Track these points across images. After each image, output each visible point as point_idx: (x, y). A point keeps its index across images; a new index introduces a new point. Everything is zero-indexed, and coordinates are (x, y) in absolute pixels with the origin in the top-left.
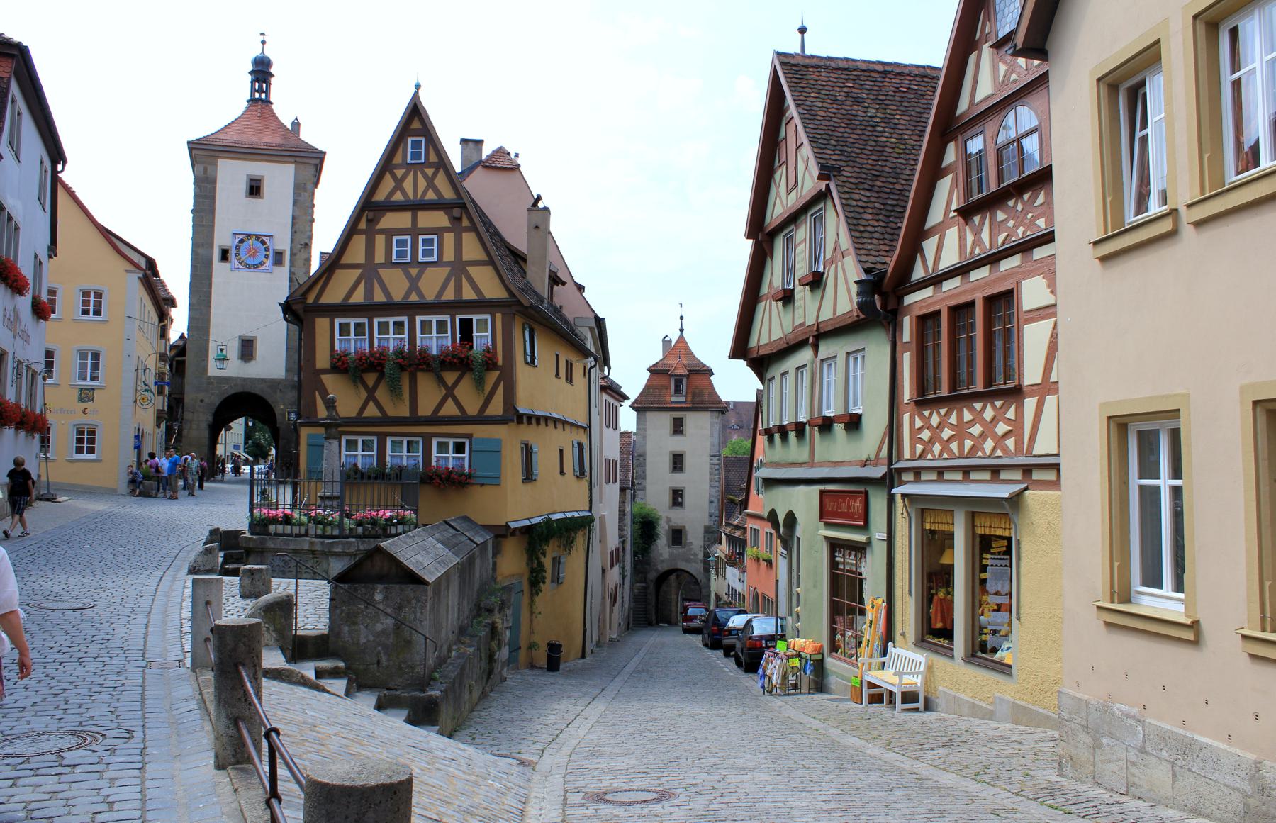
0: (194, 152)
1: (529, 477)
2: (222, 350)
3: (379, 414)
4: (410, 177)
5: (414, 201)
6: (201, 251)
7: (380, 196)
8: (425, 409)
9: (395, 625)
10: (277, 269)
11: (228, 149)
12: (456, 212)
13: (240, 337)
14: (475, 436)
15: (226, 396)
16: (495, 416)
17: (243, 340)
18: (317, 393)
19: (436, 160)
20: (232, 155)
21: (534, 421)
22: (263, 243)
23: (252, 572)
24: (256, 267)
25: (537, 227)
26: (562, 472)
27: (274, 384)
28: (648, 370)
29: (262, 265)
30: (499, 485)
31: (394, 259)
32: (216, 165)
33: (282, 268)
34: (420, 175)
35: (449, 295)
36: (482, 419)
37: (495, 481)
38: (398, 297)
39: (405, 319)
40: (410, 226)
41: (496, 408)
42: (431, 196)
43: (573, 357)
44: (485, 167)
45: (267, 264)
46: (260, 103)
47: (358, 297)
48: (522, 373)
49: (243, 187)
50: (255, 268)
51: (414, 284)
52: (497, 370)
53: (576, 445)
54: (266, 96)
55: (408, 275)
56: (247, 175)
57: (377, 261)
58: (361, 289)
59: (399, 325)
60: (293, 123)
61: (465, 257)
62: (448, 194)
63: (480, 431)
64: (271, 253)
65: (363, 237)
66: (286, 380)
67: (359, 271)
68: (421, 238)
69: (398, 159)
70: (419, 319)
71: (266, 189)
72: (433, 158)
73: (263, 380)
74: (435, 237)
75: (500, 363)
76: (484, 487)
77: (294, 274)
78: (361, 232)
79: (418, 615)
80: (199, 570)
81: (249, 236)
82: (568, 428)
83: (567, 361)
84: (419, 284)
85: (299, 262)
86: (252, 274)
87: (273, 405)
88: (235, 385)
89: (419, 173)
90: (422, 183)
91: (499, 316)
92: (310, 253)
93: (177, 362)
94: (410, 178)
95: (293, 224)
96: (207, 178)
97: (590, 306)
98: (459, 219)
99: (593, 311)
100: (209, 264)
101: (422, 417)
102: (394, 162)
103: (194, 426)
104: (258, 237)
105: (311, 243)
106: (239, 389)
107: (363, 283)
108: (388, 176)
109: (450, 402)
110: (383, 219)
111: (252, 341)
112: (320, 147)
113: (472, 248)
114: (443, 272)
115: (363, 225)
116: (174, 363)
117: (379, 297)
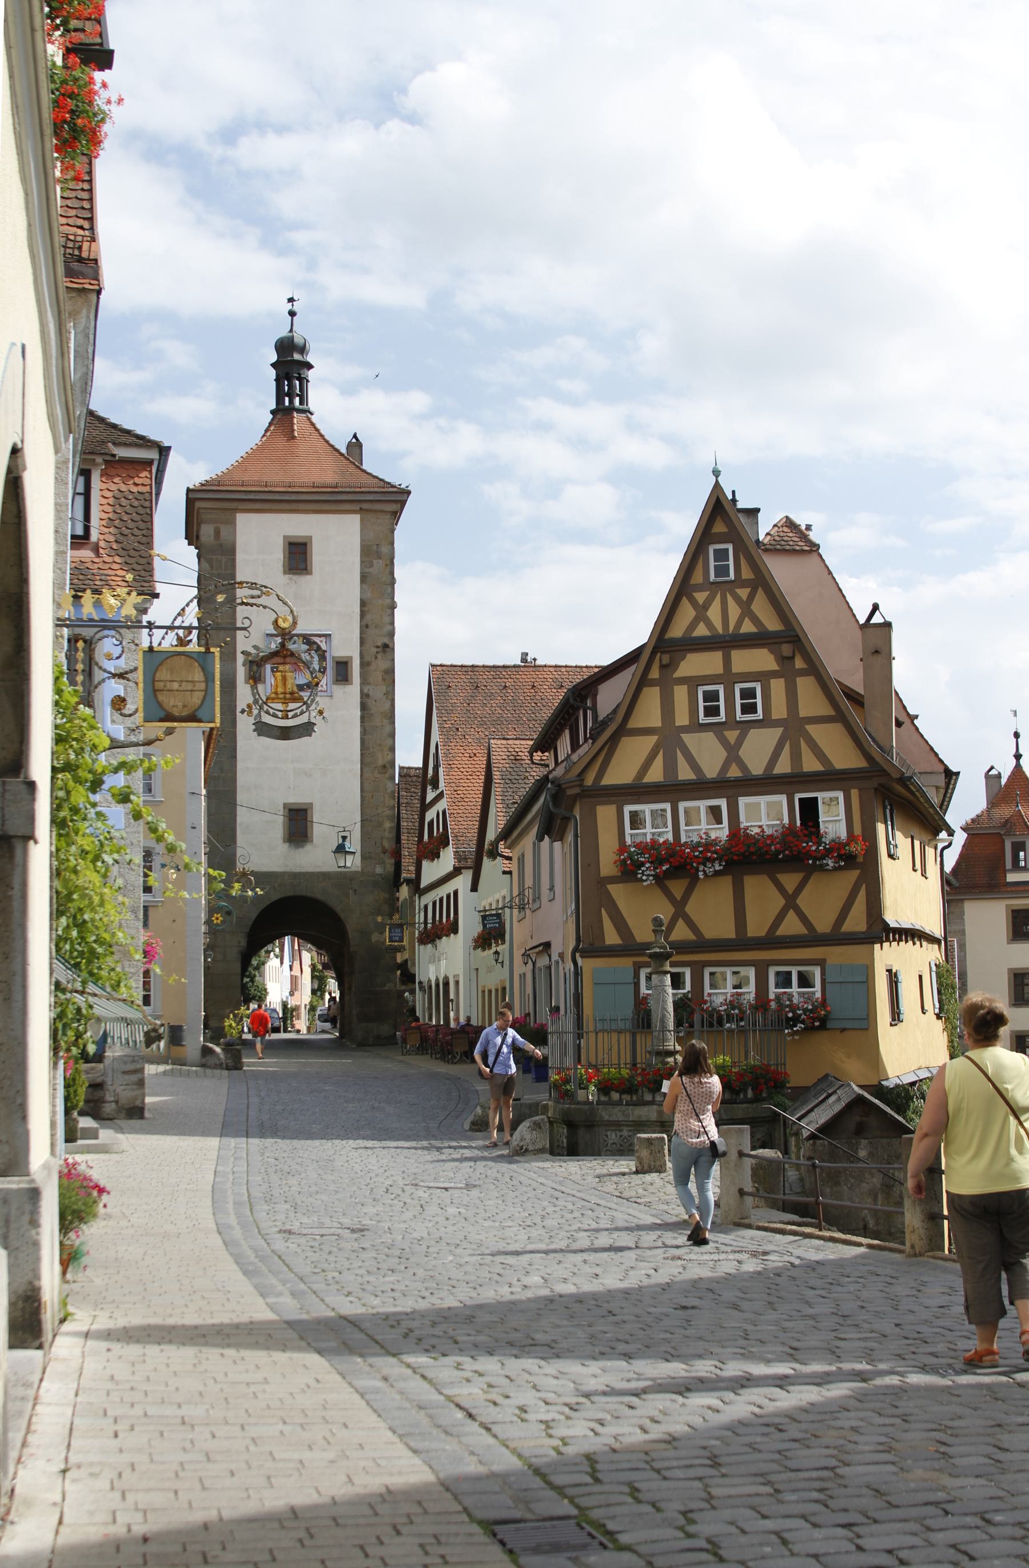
1: (896, 1017)
2: (344, 838)
4: (716, 604)
5: (723, 636)
7: (677, 631)
8: (756, 928)
10: (338, 690)
11: (252, 496)
12: (786, 649)
13: (285, 805)
15: (268, 903)
17: (290, 810)
20: (258, 506)
25: (876, 652)
27: (342, 880)
32: (233, 523)
33: (348, 688)
35: (783, 766)
36: (837, 938)
37: (867, 1024)
38: (711, 771)
39: (723, 803)
40: (720, 670)
41: (856, 922)
42: (748, 627)
45: (323, 682)
46: (295, 414)
47: (656, 774)
49: (278, 556)
51: (733, 752)
52: (857, 869)
53: (934, 968)
54: (301, 403)
55: (724, 742)
56: (284, 537)
57: (679, 722)
58: (659, 762)
59: (715, 813)
60: (350, 445)
61: (802, 713)
62: (773, 624)
63: (835, 955)
64: (330, 665)
65: (657, 689)
66: (362, 872)
67: (655, 738)
68: (738, 688)
69: (697, 578)
70: (743, 801)
71: (317, 556)
72: (747, 574)
77: (368, 696)
78: (653, 683)
80: (527, 1150)
84: (740, 753)
85: (377, 676)
87: (342, 916)
89: (729, 597)
90: (734, 611)
91: (854, 793)
92: (393, 660)
94: (716, 604)
95: (363, 615)
97: (936, 755)
98: (792, 658)
101: (753, 938)
102: (693, 582)
106: (290, 893)
107: (661, 753)
108: (685, 602)
109: (791, 914)
110: (682, 664)
111: (306, 810)
114: (770, 737)
115: (655, 673)
117: (685, 773)
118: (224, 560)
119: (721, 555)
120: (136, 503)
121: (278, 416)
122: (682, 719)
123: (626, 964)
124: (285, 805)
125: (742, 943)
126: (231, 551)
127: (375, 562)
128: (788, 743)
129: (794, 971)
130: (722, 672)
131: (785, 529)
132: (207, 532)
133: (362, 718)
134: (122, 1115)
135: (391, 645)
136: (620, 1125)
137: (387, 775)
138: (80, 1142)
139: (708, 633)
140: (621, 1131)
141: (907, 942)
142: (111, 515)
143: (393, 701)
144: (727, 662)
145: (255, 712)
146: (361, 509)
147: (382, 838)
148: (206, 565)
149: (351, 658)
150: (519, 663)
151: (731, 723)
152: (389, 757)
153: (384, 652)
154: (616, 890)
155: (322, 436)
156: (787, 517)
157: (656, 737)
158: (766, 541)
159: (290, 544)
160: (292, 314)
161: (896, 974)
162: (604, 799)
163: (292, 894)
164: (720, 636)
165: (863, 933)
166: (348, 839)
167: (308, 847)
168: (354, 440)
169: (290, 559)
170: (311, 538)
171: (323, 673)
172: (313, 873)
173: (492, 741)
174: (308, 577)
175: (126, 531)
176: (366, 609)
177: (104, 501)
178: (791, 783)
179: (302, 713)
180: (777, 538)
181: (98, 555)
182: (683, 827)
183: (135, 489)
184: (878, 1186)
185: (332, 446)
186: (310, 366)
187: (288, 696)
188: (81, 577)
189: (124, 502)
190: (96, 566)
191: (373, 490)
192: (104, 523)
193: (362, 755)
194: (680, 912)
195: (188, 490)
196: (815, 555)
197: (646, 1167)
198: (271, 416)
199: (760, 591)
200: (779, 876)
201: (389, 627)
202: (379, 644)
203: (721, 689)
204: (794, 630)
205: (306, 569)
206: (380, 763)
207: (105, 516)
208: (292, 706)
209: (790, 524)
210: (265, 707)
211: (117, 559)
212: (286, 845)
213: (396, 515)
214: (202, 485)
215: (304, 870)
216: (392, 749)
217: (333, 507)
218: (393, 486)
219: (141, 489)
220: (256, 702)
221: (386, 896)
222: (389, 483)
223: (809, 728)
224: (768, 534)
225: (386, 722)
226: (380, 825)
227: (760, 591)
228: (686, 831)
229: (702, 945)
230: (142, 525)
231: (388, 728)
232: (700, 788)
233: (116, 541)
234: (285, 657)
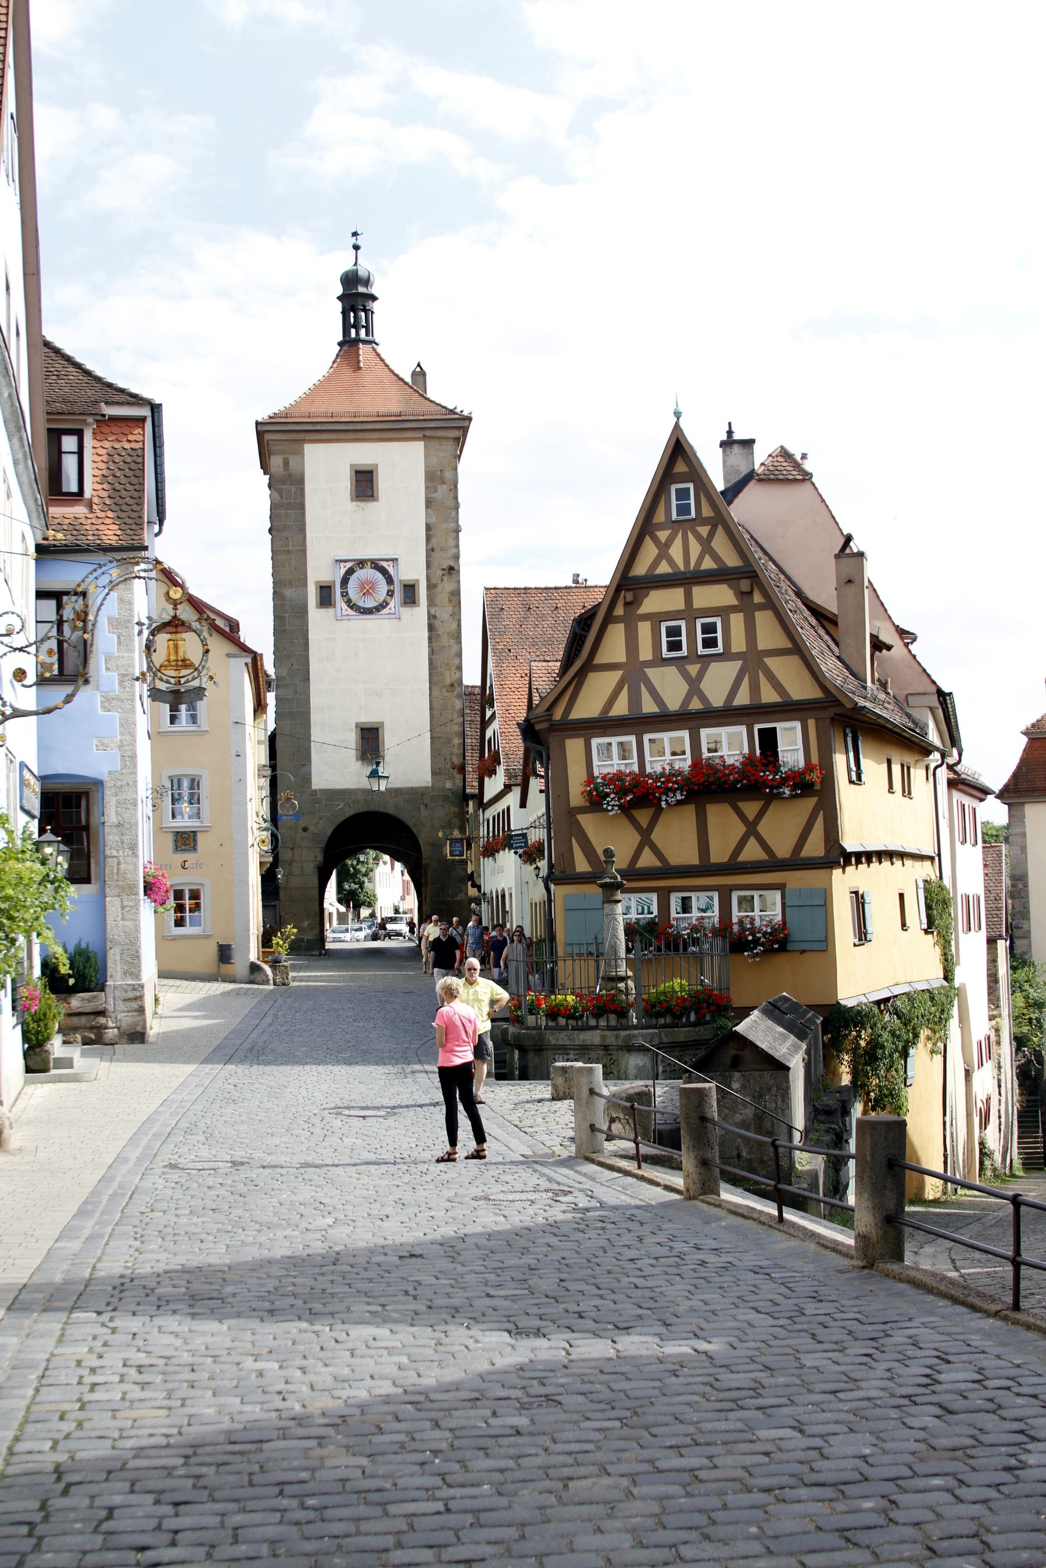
1: (862, 935)
3: (658, 864)
4: (678, 543)
5: (685, 573)
6: (289, 593)
7: (640, 569)
8: (719, 854)
9: (756, 1115)
10: (406, 612)
11: (318, 427)
12: (745, 585)
14: (788, 887)
15: (342, 819)
16: (814, 858)
19: (712, 514)
22: (384, 571)
23: (564, 1069)
25: (850, 581)
26: (904, 925)
27: (414, 795)
28: (1025, 733)
32: (301, 453)
33: (416, 610)
35: (743, 698)
36: (796, 863)
38: (674, 704)
39: (685, 734)
40: (682, 607)
41: (815, 847)
42: (708, 564)
43: (909, 758)
44: (760, 480)
45: (392, 605)
46: (361, 345)
47: (621, 708)
48: (845, 793)
49: (345, 484)
52: (814, 796)
53: (921, 885)
54: (367, 334)
55: (686, 675)
58: (624, 695)
60: (414, 374)
62: (732, 560)
63: (795, 879)
64: (397, 588)
68: (699, 623)
69: (660, 517)
71: (383, 483)
72: (707, 512)
76: (805, 955)
77: (435, 617)
78: (617, 620)
79: (779, 1103)
81: (361, 563)
82: (908, 862)
83: (902, 766)
85: (442, 597)
86: (369, 622)
87: (415, 830)
88: (354, 802)
89: (690, 535)
90: (695, 548)
91: (811, 723)
92: (459, 582)
94: (678, 543)
95: (428, 539)
96: (290, 475)
97: (929, 676)
98: (751, 593)
99: (934, 682)
100: (302, 612)
101: (716, 864)
102: (655, 521)
106: (363, 809)
107: (626, 687)
108: (648, 541)
109: (752, 842)
111: (377, 729)
113: (768, 635)
115: (619, 611)
117: (649, 706)
119: (683, 494)
120: (129, 459)
121: (345, 348)
122: (646, 653)
123: (593, 891)
125: (705, 869)
126: (298, 481)
127: (439, 487)
130: (683, 607)
131: (780, 459)
132: (276, 462)
133: (430, 639)
134: (124, 1040)
136: (567, 1049)
137: (455, 693)
138: (53, 1072)
140: (568, 1054)
141: (880, 862)
142: (104, 472)
143: (459, 621)
144: (688, 598)
145: (149, 679)
147: (451, 754)
148: (277, 495)
149: (418, 580)
150: (570, 584)
151: (694, 657)
152: (457, 676)
153: (450, 574)
154: (586, 821)
155: (387, 366)
156: (782, 447)
157: (621, 672)
158: (759, 472)
159: (357, 472)
160: (356, 248)
161: (862, 897)
168: (418, 369)
169: (357, 487)
171: (392, 596)
173: (533, 664)
174: (374, 503)
175: (118, 486)
177: (98, 459)
179: (193, 679)
180: (771, 468)
181: (91, 510)
182: (648, 758)
183: (128, 446)
184: (751, 1116)
185: (397, 376)
186: (374, 298)
187: (180, 663)
188: (75, 533)
189: (117, 458)
190: (89, 521)
192: (98, 479)
193: (430, 674)
194: (646, 840)
195: (257, 423)
196: (807, 484)
197: (561, 1094)
198: (339, 348)
199: (720, 530)
200: (740, 804)
202: (445, 567)
203: (683, 624)
204: (751, 565)
206: (448, 682)
207: (99, 473)
208: (184, 672)
209: (785, 453)
210: (159, 674)
211: (110, 514)
212: (360, 762)
213: (460, 441)
214: (271, 418)
216: (459, 668)
219: (134, 445)
220: (149, 668)
221: (456, 810)
223: (769, 661)
224: (762, 464)
225: (453, 642)
226: (449, 741)
227: (720, 530)
228: (651, 762)
229: (668, 871)
230: (134, 480)
231: (455, 648)
232: (665, 720)
233: (109, 497)
234: (176, 626)
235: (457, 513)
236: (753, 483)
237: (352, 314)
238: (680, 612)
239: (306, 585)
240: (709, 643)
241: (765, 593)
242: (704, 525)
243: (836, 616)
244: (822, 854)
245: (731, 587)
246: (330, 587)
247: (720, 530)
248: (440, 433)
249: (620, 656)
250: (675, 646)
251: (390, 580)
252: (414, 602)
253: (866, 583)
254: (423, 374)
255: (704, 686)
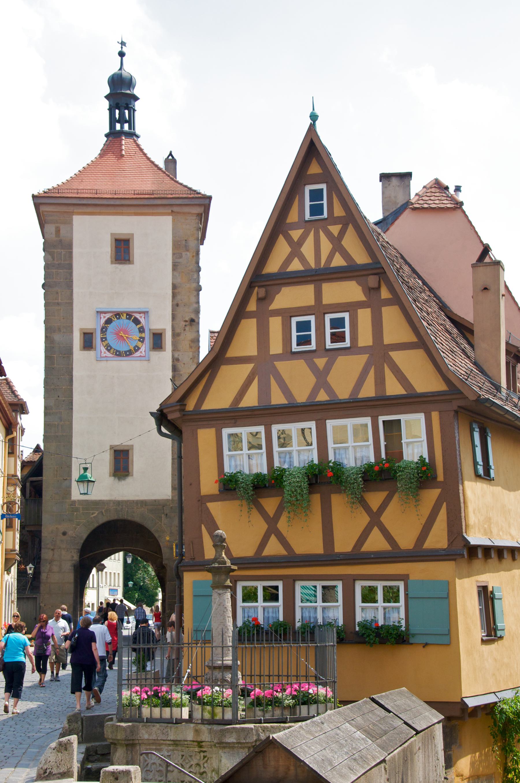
0: (43, 208)
2: (86, 469)
4: (310, 241)
5: (316, 270)
6: (57, 337)
10: (155, 355)
12: (372, 281)
13: (111, 447)
14: (411, 578)
15: (96, 525)
18: (203, 527)
20: (90, 210)
21: (493, 554)
22: (137, 322)
24: (129, 353)
25: (486, 289)
29: (136, 351)
30: (448, 645)
31: (295, 348)
34: (323, 236)
42: (338, 261)
45: (143, 349)
50: (127, 356)
54: (130, 128)
55: (313, 368)
58: (254, 388)
60: (167, 161)
61: (388, 340)
64: (147, 335)
65: (254, 320)
69: (293, 217)
70: (331, 424)
72: (339, 211)
73: (143, 503)
74: (346, 316)
75: (440, 477)
77: (178, 360)
78: (251, 315)
84: (327, 379)
85: (184, 344)
86: (124, 363)
89: (322, 234)
90: (326, 246)
91: (435, 416)
92: (198, 331)
93: (32, 482)
94: (310, 241)
95: (174, 296)
96: (61, 241)
98: (378, 289)
100: (68, 353)
102: (289, 221)
103: (55, 568)
104: (129, 315)
105: (199, 318)
106: (113, 516)
108: (281, 241)
109: (376, 532)
112: (205, 191)
115: (252, 306)
116: (28, 484)
118: (63, 253)
121: (110, 139)
124: (111, 447)
127: (184, 254)
128: (373, 369)
129: (380, 585)
135: (196, 320)
139: (301, 268)
146: (172, 211)
148: (50, 257)
149: (165, 329)
153: (191, 325)
155: (145, 155)
158: (413, 201)
159: (116, 240)
162: (205, 423)
163: (116, 518)
164: (312, 270)
165: (444, 550)
166: (89, 470)
167: (129, 480)
168: (170, 157)
170: (133, 235)
172: (133, 502)
174: (131, 266)
176: (176, 291)
178: (374, 406)
185: (153, 163)
186: (136, 99)
191: (181, 196)
198: (106, 139)
199: (351, 228)
201: (196, 306)
202: (187, 319)
203: (312, 319)
205: (129, 260)
214: (45, 192)
215: (125, 499)
217: (150, 210)
218: (200, 193)
222: (195, 191)
223: (395, 355)
224: (417, 195)
227: (351, 228)
235: (199, 275)
236: (407, 212)
237: (117, 112)
238: (309, 307)
239: (72, 332)
240: (338, 337)
241: (391, 289)
242: (335, 224)
243: (473, 324)
244: (446, 546)
245: (359, 284)
246: (92, 334)
247: (350, 230)
248: (186, 209)
249: (252, 350)
250: (304, 341)
251: (142, 330)
252: (162, 348)
253: (503, 291)
254: (174, 161)
255: (332, 379)
